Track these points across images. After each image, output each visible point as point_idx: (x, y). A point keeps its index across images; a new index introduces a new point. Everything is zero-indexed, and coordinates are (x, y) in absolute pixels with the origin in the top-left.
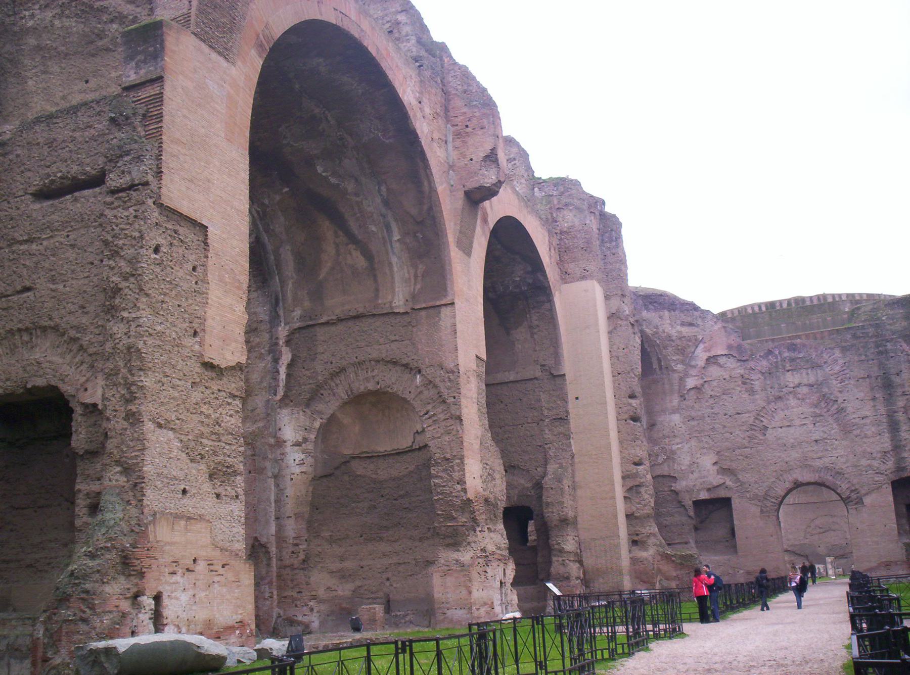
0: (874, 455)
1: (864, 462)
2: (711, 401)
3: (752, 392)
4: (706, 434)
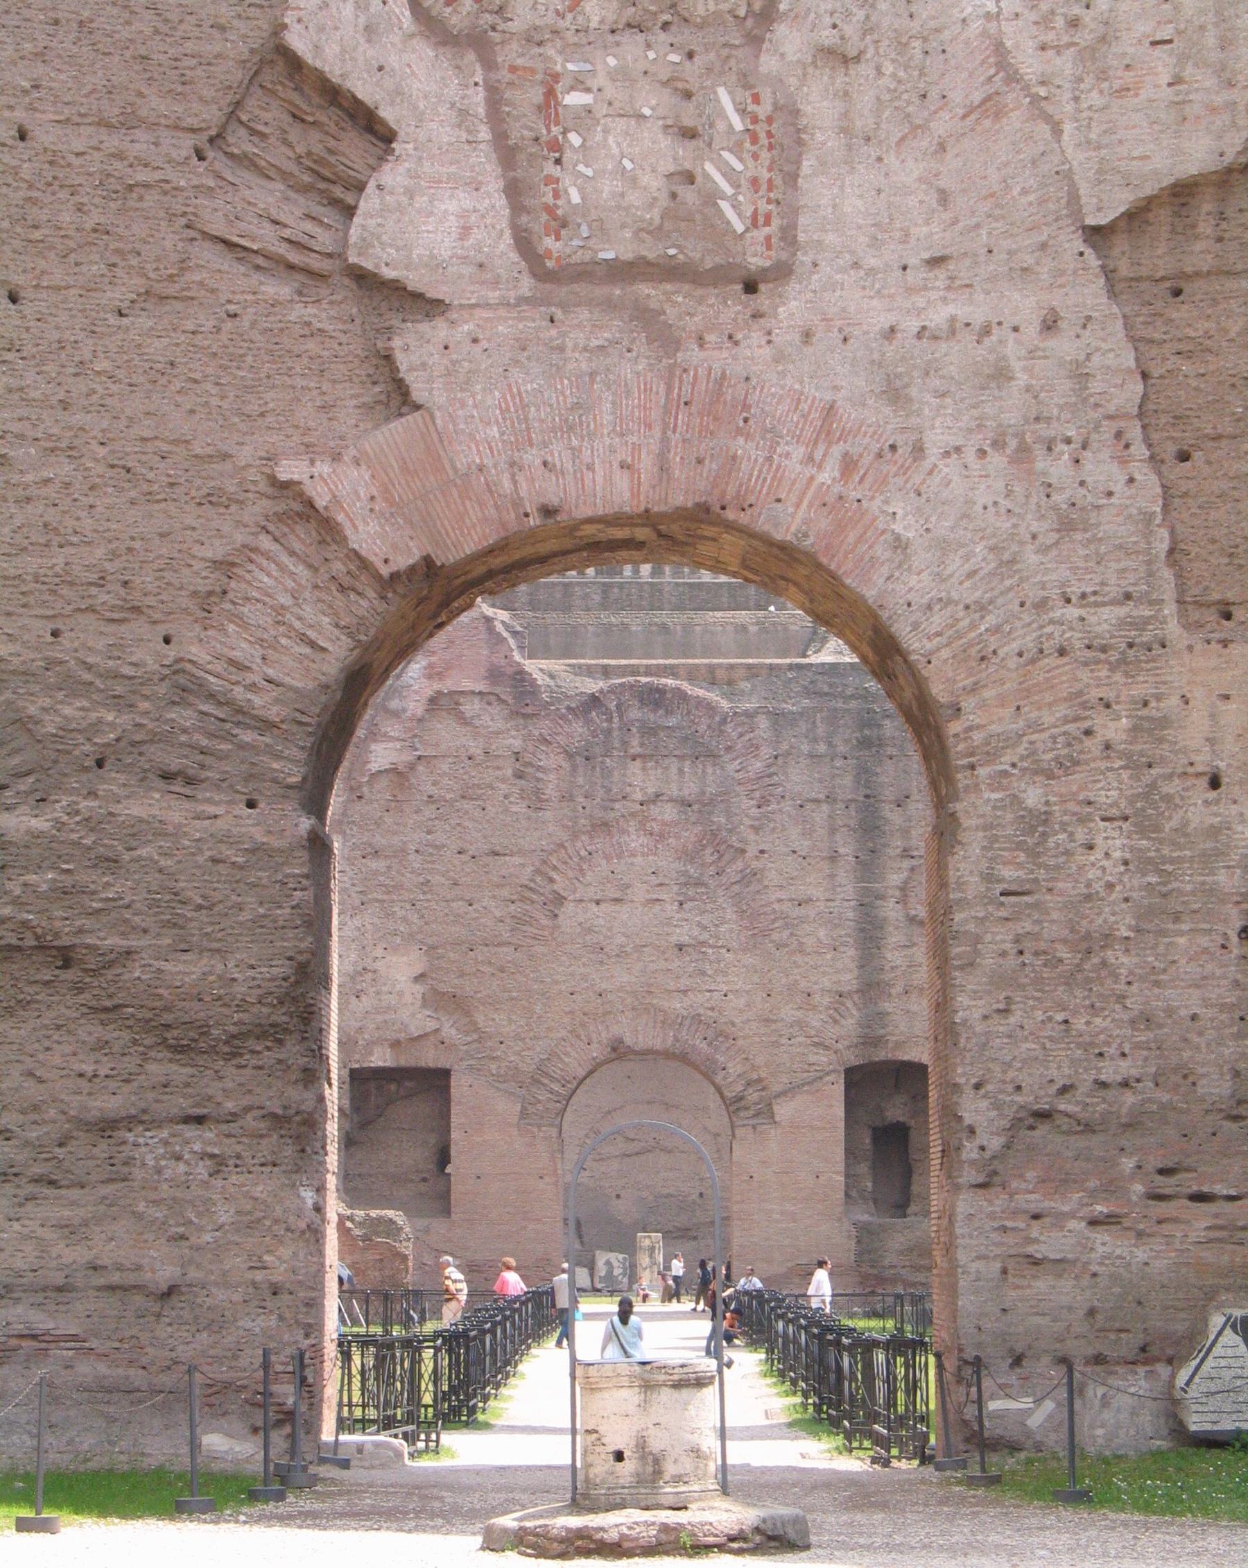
0: (816, 998)
1: (788, 1012)
2: (429, 811)
3: (537, 801)
4: (406, 896)
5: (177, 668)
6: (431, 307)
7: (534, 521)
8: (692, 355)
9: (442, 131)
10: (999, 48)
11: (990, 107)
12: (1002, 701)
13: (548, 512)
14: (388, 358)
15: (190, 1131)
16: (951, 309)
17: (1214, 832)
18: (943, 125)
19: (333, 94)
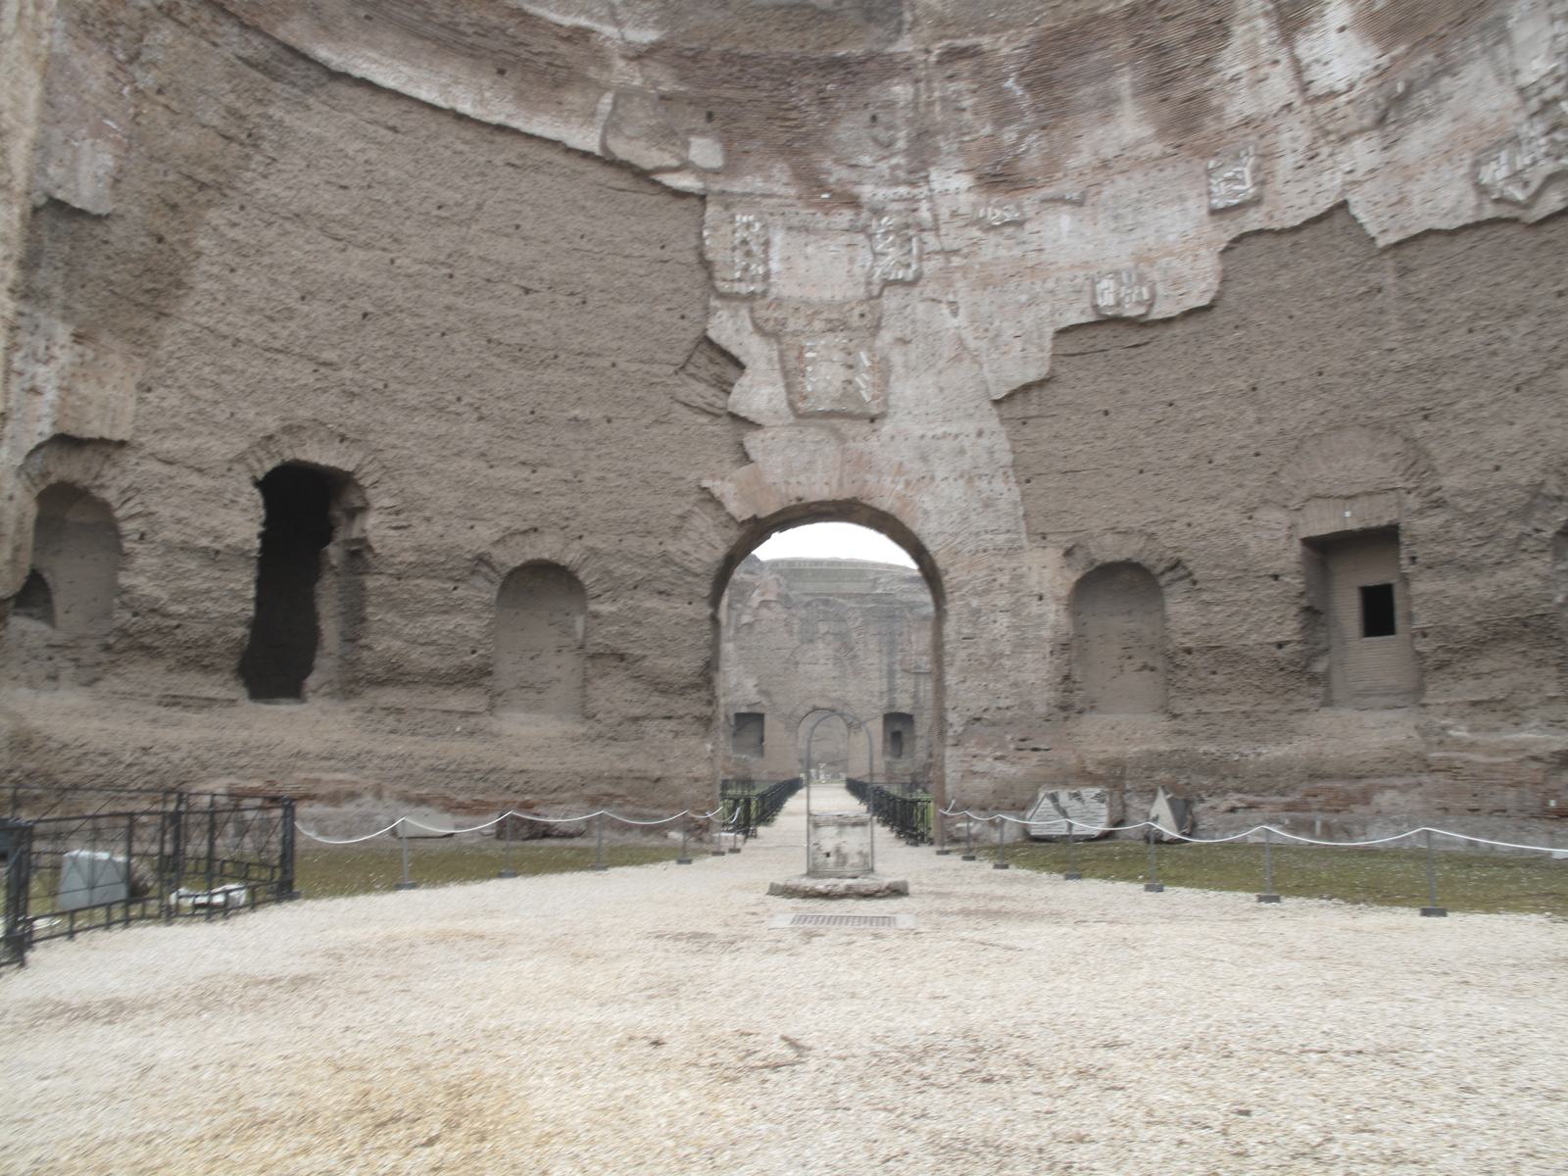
1: (866, 698)
3: (791, 633)
5: (664, 554)
6: (758, 426)
7: (794, 503)
9: (762, 365)
11: (957, 359)
12: (963, 568)
13: (799, 499)
14: (741, 445)
15: (666, 722)
17: (1040, 616)
18: (941, 364)
19: (725, 353)
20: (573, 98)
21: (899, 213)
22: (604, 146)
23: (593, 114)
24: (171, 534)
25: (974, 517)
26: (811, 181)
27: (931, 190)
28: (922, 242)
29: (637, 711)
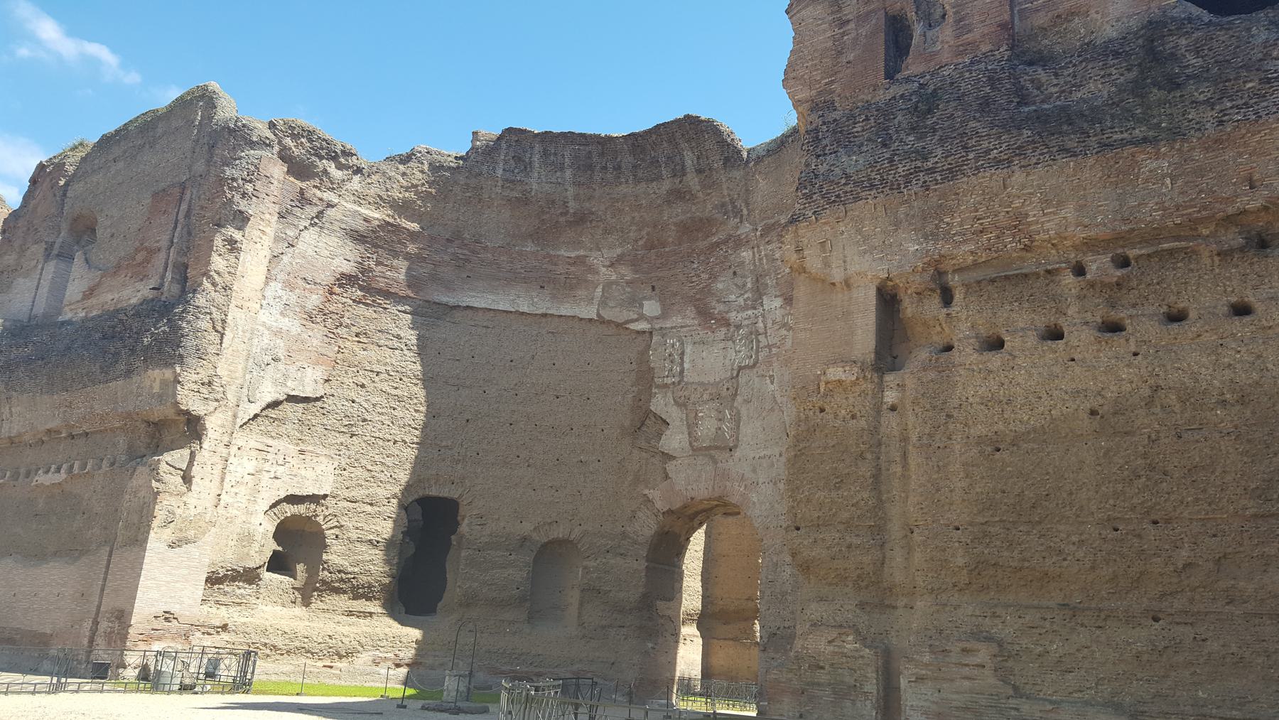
6: (674, 458)
8: (720, 465)
9: (677, 423)
10: (775, 397)
11: (772, 410)
13: (692, 499)
16: (764, 452)
20: (581, 293)
21: (747, 326)
22: (598, 315)
23: (592, 299)
24: (354, 535)
25: (776, 506)
26: (704, 314)
27: (764, 310)
28: (758, 341)
29: (604, 623)
